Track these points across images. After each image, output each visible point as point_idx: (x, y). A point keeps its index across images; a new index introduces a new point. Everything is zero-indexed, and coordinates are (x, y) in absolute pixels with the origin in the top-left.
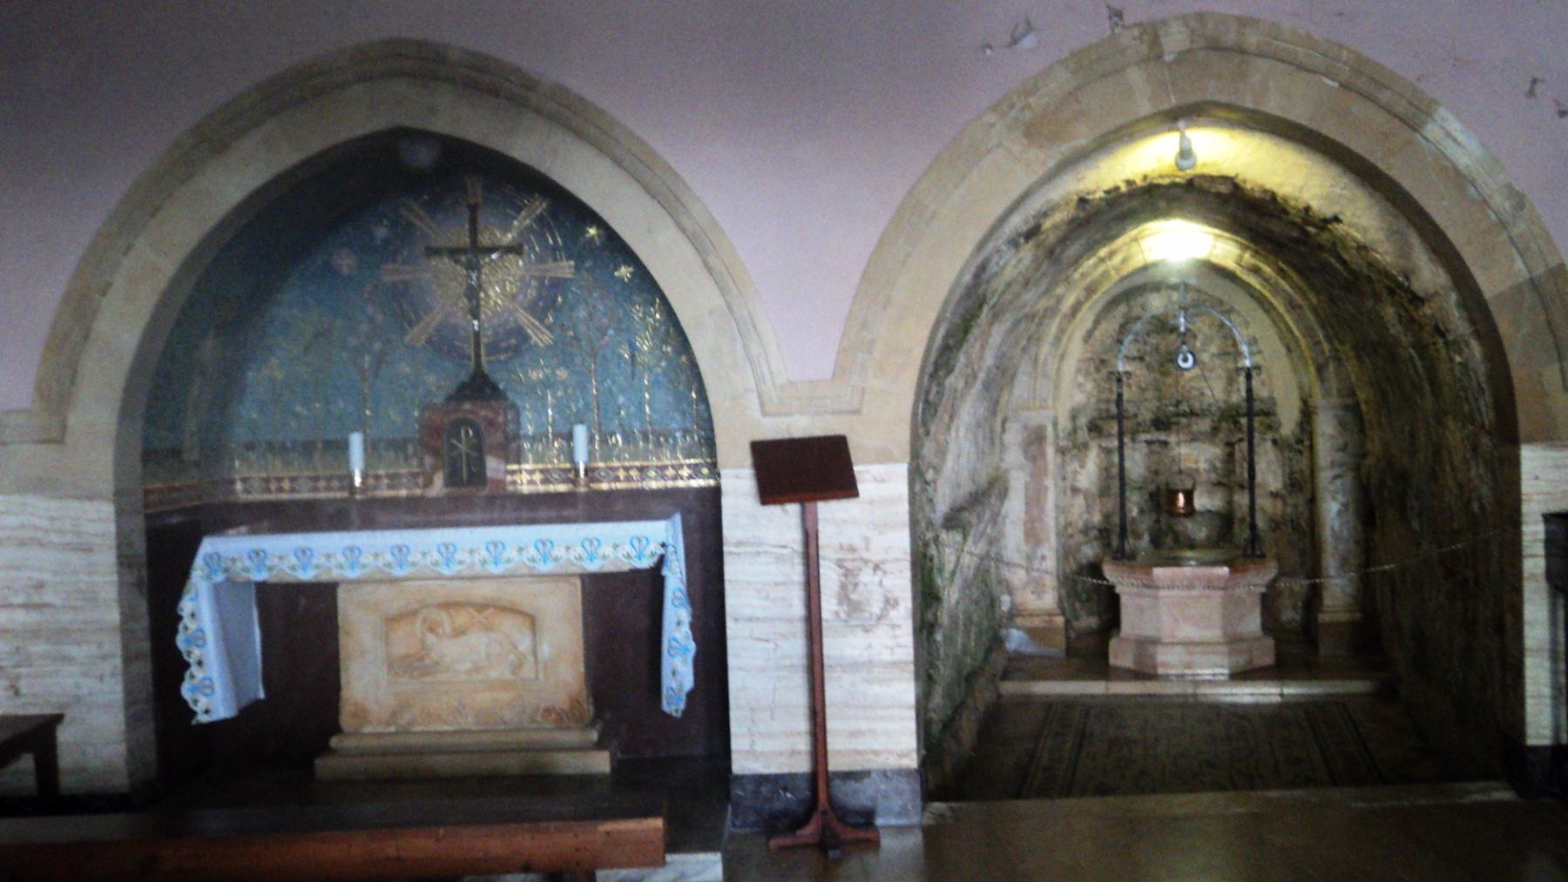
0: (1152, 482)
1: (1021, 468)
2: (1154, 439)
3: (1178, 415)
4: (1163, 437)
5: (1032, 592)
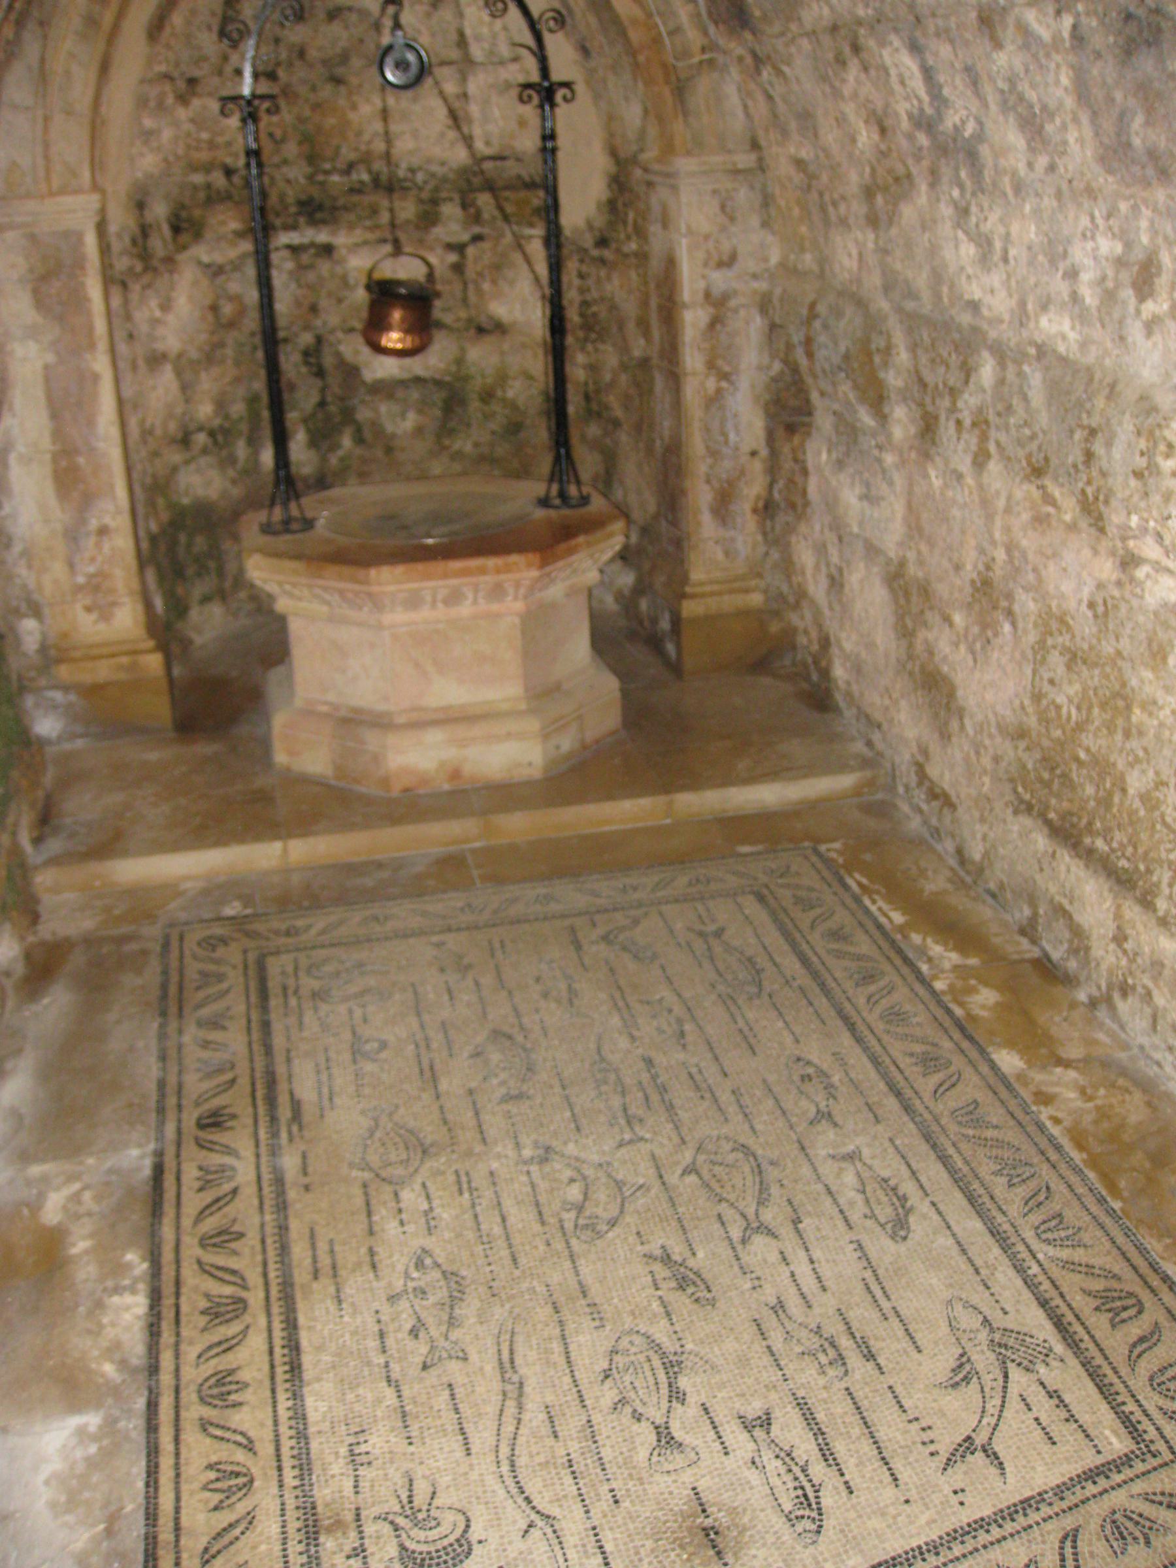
0: (307, 327)
1: (32, 333)
2: (306, 241)
3: (355, 190)
4: (323, 237)
5: (88, 609)
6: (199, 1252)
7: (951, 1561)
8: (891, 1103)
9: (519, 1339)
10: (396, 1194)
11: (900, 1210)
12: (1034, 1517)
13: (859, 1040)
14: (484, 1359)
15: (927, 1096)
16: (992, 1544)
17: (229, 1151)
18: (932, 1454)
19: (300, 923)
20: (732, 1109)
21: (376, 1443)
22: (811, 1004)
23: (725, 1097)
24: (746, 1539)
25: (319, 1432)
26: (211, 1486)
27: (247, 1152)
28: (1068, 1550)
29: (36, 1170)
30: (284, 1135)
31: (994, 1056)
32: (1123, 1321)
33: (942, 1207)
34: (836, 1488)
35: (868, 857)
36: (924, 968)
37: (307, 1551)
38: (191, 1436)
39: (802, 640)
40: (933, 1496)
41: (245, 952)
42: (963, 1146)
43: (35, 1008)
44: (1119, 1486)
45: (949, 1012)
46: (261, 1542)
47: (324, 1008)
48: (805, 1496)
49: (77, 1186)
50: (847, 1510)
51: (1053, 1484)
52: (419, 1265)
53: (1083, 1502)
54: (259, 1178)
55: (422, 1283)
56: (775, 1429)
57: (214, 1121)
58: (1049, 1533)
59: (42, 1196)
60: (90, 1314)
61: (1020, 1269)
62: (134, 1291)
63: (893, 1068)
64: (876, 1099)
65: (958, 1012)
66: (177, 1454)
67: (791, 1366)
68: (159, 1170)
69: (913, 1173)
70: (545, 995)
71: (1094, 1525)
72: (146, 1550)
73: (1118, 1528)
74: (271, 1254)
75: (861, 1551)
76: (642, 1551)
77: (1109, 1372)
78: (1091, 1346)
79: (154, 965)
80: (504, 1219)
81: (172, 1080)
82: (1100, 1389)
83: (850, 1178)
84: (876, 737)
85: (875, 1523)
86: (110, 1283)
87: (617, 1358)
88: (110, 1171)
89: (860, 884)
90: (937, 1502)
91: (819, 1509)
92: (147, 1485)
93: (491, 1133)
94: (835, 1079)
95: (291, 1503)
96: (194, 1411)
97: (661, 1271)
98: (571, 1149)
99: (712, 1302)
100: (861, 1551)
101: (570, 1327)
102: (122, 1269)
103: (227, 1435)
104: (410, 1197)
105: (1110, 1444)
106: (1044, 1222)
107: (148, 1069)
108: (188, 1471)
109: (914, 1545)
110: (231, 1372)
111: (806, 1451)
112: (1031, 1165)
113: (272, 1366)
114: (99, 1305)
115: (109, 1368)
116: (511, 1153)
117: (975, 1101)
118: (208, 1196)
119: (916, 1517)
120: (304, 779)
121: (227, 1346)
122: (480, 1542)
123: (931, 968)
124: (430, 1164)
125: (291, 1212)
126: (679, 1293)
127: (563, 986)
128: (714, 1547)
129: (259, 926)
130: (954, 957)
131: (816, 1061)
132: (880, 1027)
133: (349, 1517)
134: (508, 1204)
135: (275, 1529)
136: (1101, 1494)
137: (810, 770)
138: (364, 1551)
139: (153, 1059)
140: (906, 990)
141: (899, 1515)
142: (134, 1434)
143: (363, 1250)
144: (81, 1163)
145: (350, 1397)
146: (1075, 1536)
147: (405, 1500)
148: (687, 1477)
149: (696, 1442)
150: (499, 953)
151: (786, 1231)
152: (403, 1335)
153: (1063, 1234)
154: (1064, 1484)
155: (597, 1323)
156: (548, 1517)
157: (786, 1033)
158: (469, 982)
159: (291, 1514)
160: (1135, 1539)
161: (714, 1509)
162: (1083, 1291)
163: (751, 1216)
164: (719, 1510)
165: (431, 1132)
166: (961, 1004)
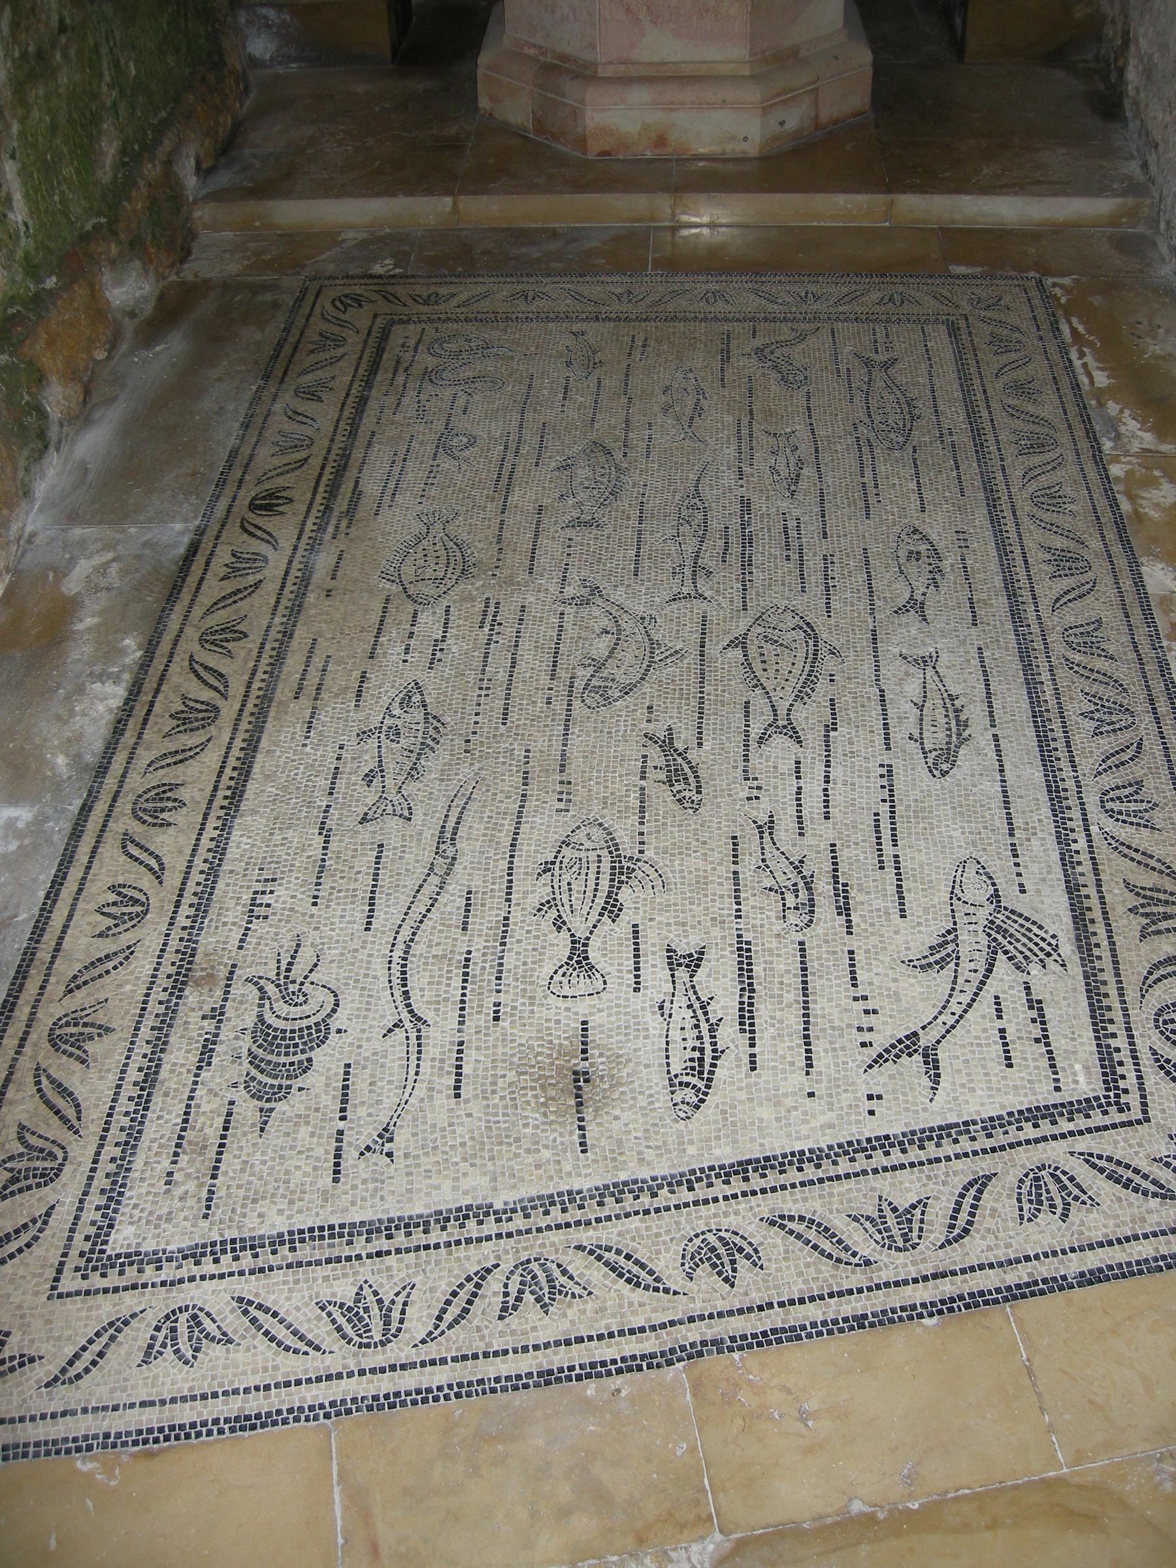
6: (196, 647)
7: (830, 1179)
8: (1001, 603)
9: (473, 806)
10: (415, 616)
11: (954, 738)
12: (948, 1149)
13: (995, 521)
14: (426, 825)
15: (1045, 603)
16: (885, 1169)
17: (270, 539)
18: (863, 1045)
19: (443, 291)
20: (815, 579)
21: (281, 897)
22: (957, 468)
23: (813, 563)
24: (615, 1096)
25: (231, 872)
26: (105, 910)
27: (286, 544)
28: (968, 1200)
29: (78, 532)
30: (331, 529)
31: (1144, 569)
32: (1159, 932)
33: (1003, 743)
34: (739, 1059)
35: (1097, 300)
36: (1107, 445)
37: (168, 1001)
38: (110, 851)
39: (1109, 31)
40: (844, 1095)
41: (375, 316)
42: (1062, 673)
43: (144, 353)
44: (1063, 1136)
45: (1114, 505)
46: (128, 981)
47: (429, 388)
48: (701, 1060)
49: (110, 555)
50: (740, 1089)
51: (985, 1116)
52: (406, 702)
53: (1011, 1146)
54: (287, 573)
55: (399, 723)
56: (701, 973)
57: (267, 504)
58: (955, 1173)
59: (73, 562)
60: (68, 698)
61: (1063, 839)
62: (117, 680)
63: (1019, 561)
64: (984, 596)
65: (1125, 506)
66: (88, 868)
67: (751, 902)
68: (193, 549)
69: (989, 694)
70: (666, 409)
71: (1012, 1179)
72: (20, 966)
73: (1038, 1187)
74: (265, 660)
75: (735, 1141)
76: (500, 1081)
77: (1113, 992)
78: (1106, 955)
79: (281, 319)
80: (514, 664)
81: (246, 451)
82: (1093, 1011)
83: (913, 688)
84: (1152, 159)
85: (766, 1113)
86: (97, 669)
87: (566, 851)
88: (146, 544)
89: (1074, 331)
90: (844, 1104)
91: (710, 1080)
92: (47, 897)
93: (542, 560)
94: (946, 564)
95: (174, 944)
96: (124, 823)
97: (656, 756)
98: (619, 596)
99: (696, 807)
100: (735, 1141)
101: (531, 804)
102: (115, 652)
103: (143, 856)
104: (430, 623)
105: (1076, 1082)
106: (1118, 788)
107: (228, 435)
108: (92, 888)
109: (797, 1149)
110: (173, 787)
111: (724, 1008)
112: (1132, 714)
113: (216, 789)
114: (80, 690)
115: (61, 760)
116: (554, 588)
117: (1099, 621)
118: (229, 587)
119: (814, 1116)
120: (505, 129)
121: (181, 757)
122: (339, 1031)
123: (1114, 448)
124: (466, 586)
125: (302, 617)
126: (667, 787)
127: (690, 401)
128: (578, 1096)
129: (401, 291)
130: (1148, 439)
131: (934, 537)
132: (1025, 507)
133: (223, 972)
134: (525, 644)
135: (148, 970)
136: (1037, 1141)
137: (1064, 188)
138: (222, 1014)
139: (237, 425)
140: (1073, 469)
141: (796, 1108)
142: (56, 838)
143: (357, 674)
144: (123, 531)
145: (277, 838)
146: (984, 1185)
147: (283, 967)
148: (582, 1008)
149: (609, 969)
150: (637, 355)
151: (813, 738)
152: (357, 778)
153: (1133, 807)
154: (1000, 1117)
155: (562, 805)
156: (419, 1019)
157: (914, 497)
158: (592, 382)
159: (170, 956)
160: (1052, 1206)
161: (596, 1052)
162: (1127, 884)
163: (782, 712)
164: (601, 1055)
165: (481, 550)
166: (1132, 498)
